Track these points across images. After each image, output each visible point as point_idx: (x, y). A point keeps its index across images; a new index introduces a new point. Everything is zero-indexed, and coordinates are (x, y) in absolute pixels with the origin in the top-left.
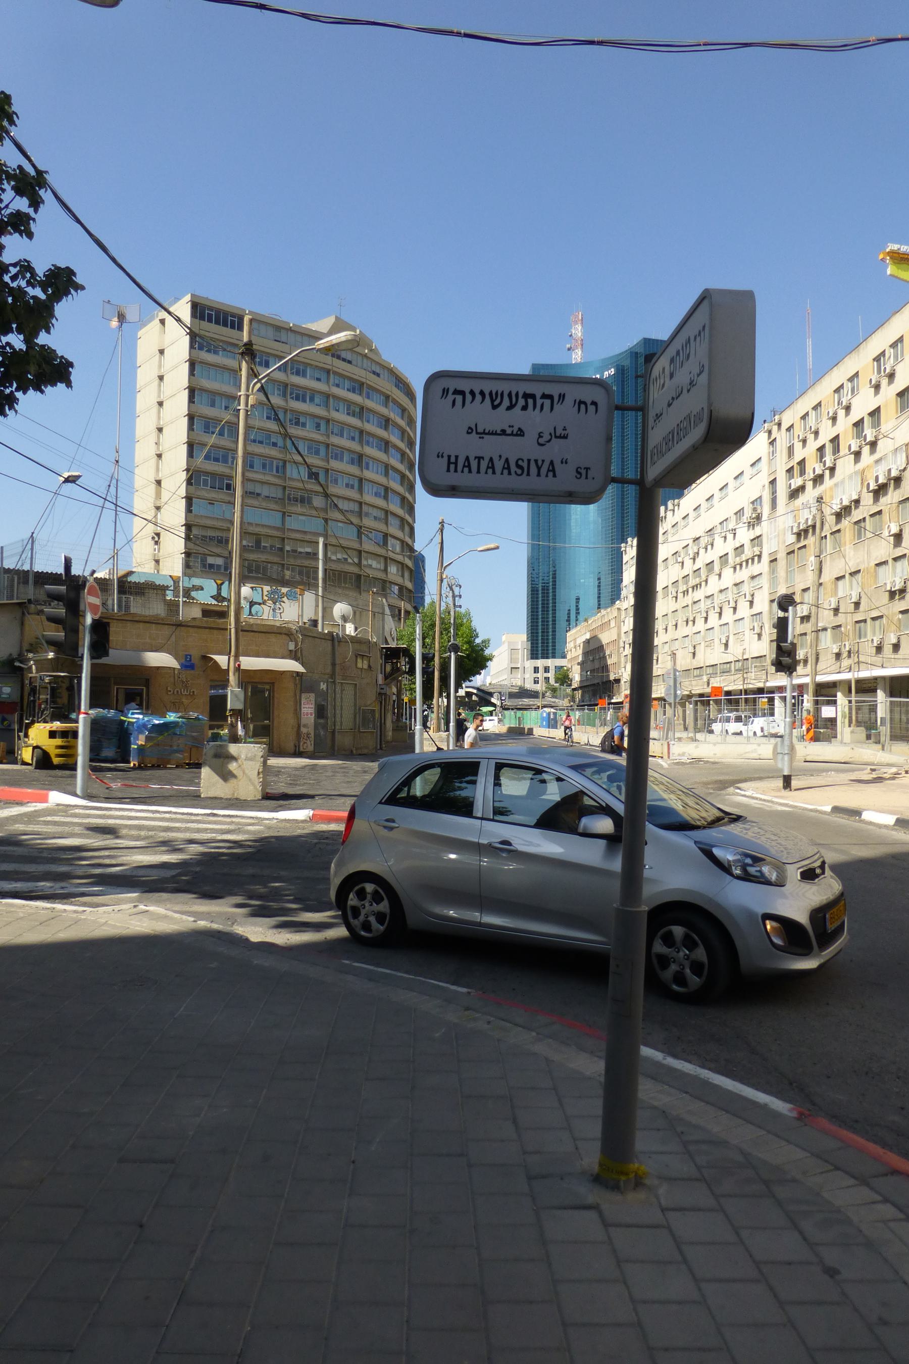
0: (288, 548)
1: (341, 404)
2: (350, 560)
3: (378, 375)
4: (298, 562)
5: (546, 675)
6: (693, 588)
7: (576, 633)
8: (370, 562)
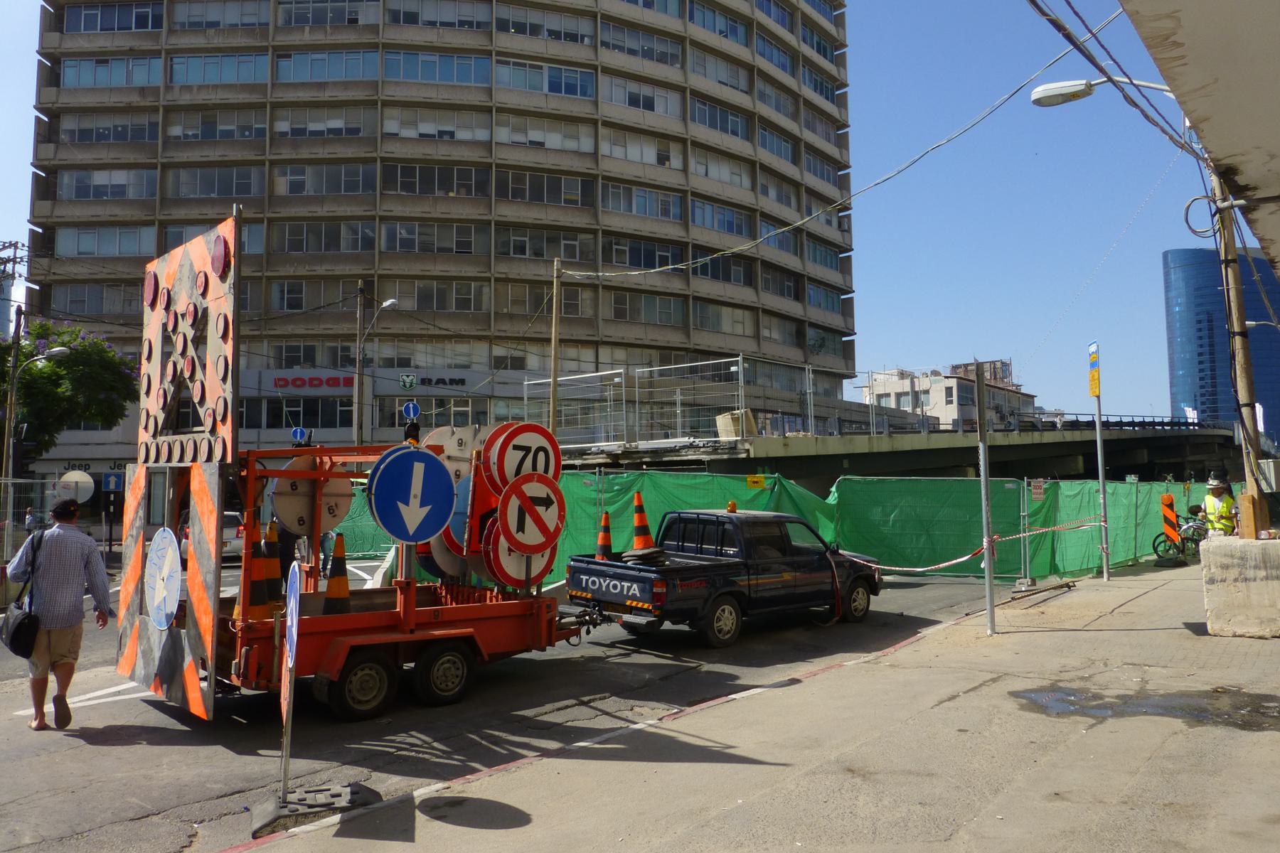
0: (283, 126)
2: (462, 135)
4: (305, 154)
8: (535, 135)
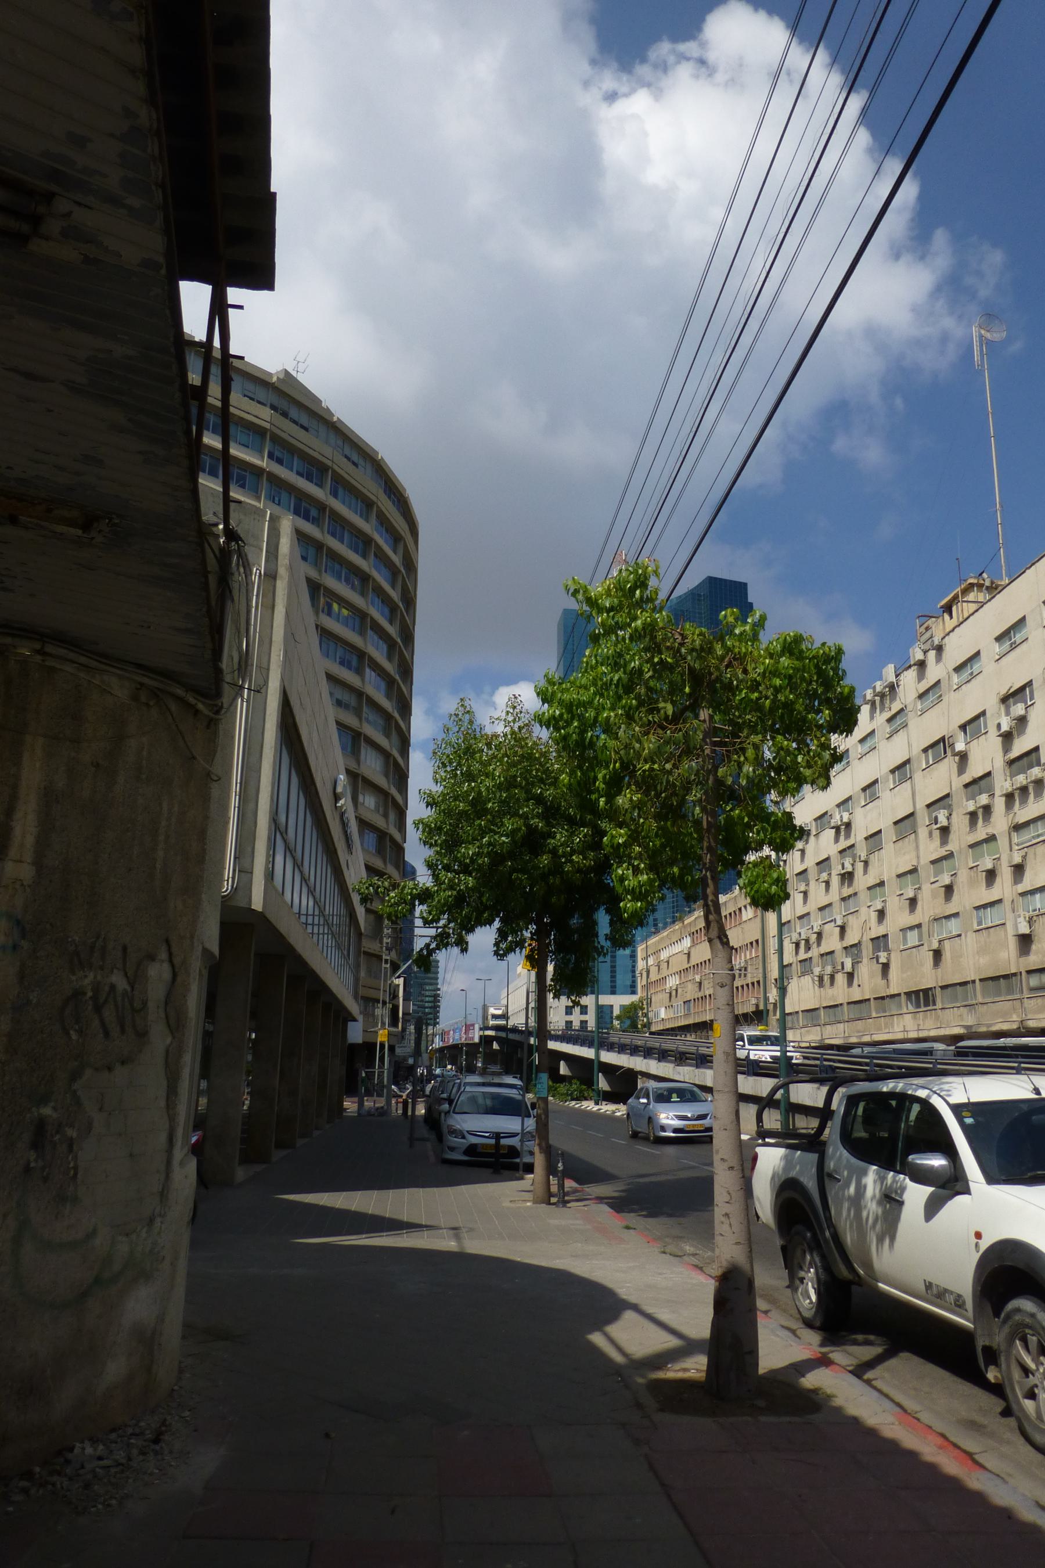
1: (284, 496)
3: (355, 464)
5: (584, 1018)
6: (1009, 797)
7: (659, 942)
